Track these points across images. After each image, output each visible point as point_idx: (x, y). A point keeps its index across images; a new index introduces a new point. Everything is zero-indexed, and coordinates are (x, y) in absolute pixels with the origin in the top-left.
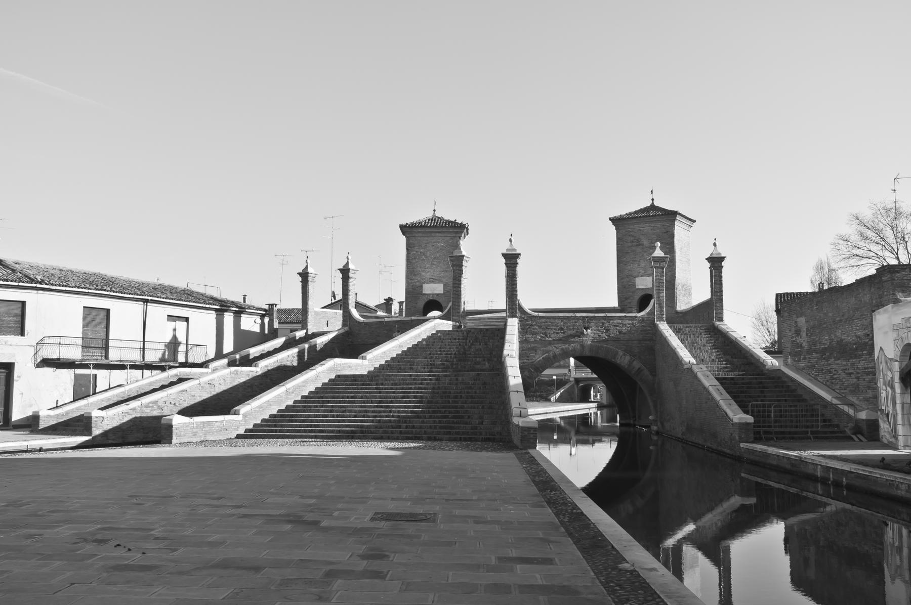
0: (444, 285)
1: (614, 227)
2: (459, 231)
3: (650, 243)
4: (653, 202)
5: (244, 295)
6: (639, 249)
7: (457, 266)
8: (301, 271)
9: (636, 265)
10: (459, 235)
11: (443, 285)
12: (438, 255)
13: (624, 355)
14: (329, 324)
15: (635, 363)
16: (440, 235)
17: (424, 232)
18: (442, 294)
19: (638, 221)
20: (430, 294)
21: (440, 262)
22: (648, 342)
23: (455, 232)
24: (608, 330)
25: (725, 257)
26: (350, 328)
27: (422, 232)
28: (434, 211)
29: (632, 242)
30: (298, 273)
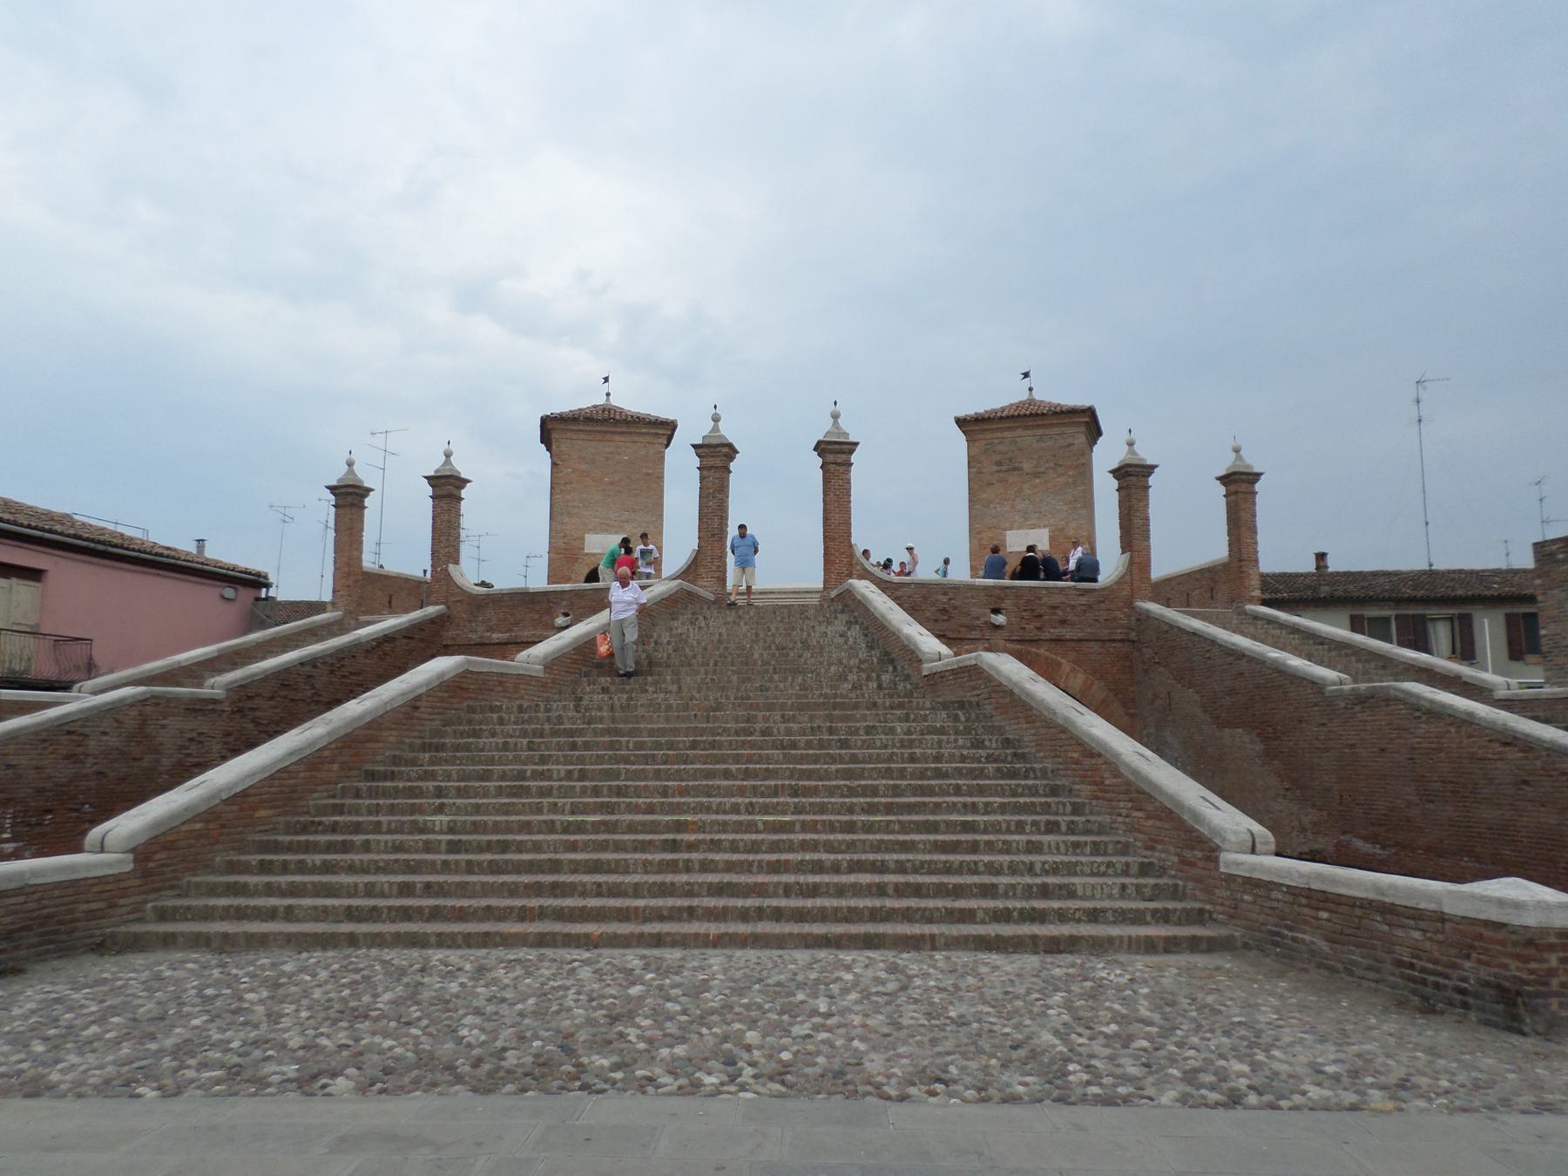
3: (1035, 467)
4: (1030, 394)
6: (1013, 478)
9: (1007, 508)
10: (660, 440)
13: (1073, 670)
14: (394, 603)
15: (1094, 688)
16: (623, 439)
19: (1011, 425)
22: (1120, 645)
23: (652, 434)
25: (1262, 474)
26: (448, 608)
28: (608, 394)
29: (999, 463)
30: (327, 487)
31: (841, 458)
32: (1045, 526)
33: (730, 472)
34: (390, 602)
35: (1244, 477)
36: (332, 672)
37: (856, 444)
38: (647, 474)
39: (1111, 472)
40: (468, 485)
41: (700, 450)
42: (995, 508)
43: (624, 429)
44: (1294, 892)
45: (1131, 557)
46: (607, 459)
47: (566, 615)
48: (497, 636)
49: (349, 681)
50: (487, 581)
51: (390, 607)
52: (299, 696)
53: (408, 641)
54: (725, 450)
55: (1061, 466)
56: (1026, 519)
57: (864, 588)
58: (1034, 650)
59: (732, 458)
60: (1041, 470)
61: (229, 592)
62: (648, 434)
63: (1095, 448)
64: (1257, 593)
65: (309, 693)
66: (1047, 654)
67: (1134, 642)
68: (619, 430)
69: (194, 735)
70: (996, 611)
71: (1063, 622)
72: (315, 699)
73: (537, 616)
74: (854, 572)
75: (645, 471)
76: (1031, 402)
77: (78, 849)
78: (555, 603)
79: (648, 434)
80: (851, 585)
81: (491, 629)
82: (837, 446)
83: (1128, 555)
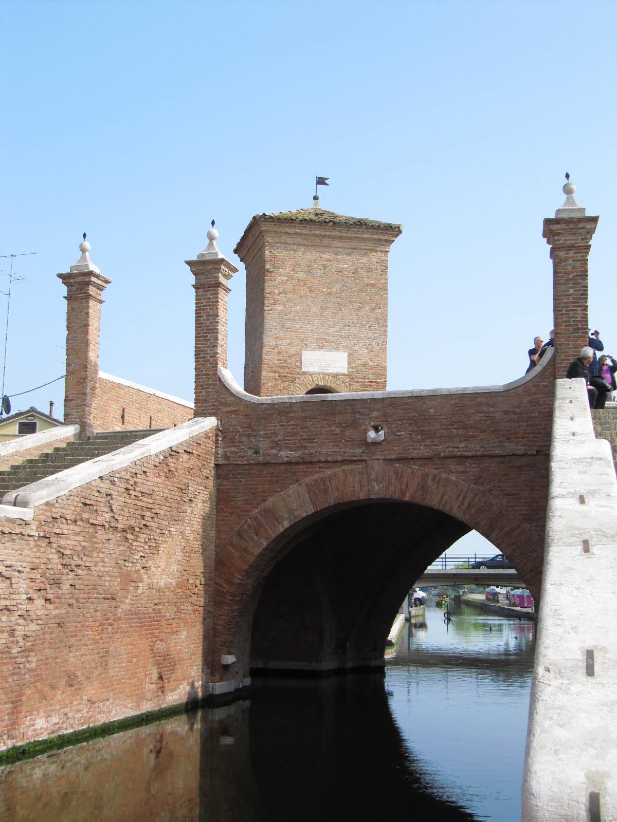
2: (386, 238)
7: (571, 247)
8: (67, 270)
10: (382, 248)
11: (346, 354)
12: (336, 288)
14: (126, 418)
16: (341, 244)
17: (306, 235)
18: (343, 374)
20: (319, 374)
21: (339, 304)
23: (375, 239)
26: (221, 420)
27: (301, 234)
30: (60, 276)
34: (123, 417)
36: (127, 489)
38: (373, 285)
46: (325, 267)
47: (377, 429)
49: (141, 504)
52: (99, 520)
53: (186, 456)
62: (370, 239)
68: (339, 234)
72: (113, 525)
73: (338, 430)
75: (367, 281)
78: (362, 414)
79: (370, 239)
81: (276, 445)
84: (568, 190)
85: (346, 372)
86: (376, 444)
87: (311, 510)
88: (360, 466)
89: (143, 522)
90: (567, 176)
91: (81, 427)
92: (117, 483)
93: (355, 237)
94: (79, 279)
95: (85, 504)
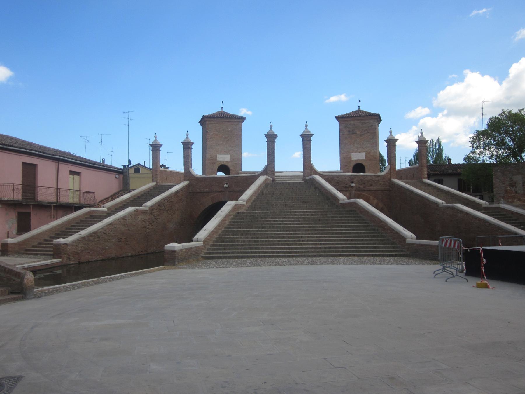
0: (231, 156)
1: (338, 123)
2: (241, 121)
3: (360, 133)
5: (102, 159)
8: (151, 143)
14: (168, 179)
18: (229, 161)
19: (353, 119)
20: (222, 161)
24: (365, 184)
26: (190, 181)
27: (217, 121)
28: (222, 108)
29: (349, 131)
31: (308, 139)
32: (364, 152)
33: (275, 142)
35: (423, 142)
36: (167, 201)
37: (313, 134)
38: (238, 135)
39: (385, 140)
40: (193, 144)
41: (267, 136)
42: (348, 146)
43: (229, 120)
44: (417, 244)
45: (390, 166)
47: (227, 184)
48: (206, 190)
50: (164, 164)
51: (167, 180)
53: (182, 192)
54: (274, 136)
55: (369, 132)
56: (358, 149)
57: (318, 178)
58: (363, 193)
59: (276, 138)
60: (363, 134)
61: (117, 176)
63: (379, 125)
64: (426, 176)
65: (163, 207)
66: (366, 194)
67: (391, 190)
68: (227, 120)
69: (143, 220)
70: (352, 182)
71: (371, 185)
74: (312, 172)
76: (359, 110)
77: (192, 241)
80: (313, 176)
82: (307, 135)
83: (390, 165)
84: (271, 126)
85: (230, 160)
86: (227, 188)
87: (212, 204)
88: (223, 193)
89: (171, 208)
90: (271, 123)
91: (156, 183)
92: (165, 200)
93: (232, 121)
94: (154, 146)
95: (159, 205)
